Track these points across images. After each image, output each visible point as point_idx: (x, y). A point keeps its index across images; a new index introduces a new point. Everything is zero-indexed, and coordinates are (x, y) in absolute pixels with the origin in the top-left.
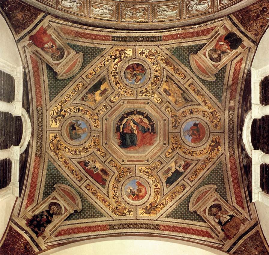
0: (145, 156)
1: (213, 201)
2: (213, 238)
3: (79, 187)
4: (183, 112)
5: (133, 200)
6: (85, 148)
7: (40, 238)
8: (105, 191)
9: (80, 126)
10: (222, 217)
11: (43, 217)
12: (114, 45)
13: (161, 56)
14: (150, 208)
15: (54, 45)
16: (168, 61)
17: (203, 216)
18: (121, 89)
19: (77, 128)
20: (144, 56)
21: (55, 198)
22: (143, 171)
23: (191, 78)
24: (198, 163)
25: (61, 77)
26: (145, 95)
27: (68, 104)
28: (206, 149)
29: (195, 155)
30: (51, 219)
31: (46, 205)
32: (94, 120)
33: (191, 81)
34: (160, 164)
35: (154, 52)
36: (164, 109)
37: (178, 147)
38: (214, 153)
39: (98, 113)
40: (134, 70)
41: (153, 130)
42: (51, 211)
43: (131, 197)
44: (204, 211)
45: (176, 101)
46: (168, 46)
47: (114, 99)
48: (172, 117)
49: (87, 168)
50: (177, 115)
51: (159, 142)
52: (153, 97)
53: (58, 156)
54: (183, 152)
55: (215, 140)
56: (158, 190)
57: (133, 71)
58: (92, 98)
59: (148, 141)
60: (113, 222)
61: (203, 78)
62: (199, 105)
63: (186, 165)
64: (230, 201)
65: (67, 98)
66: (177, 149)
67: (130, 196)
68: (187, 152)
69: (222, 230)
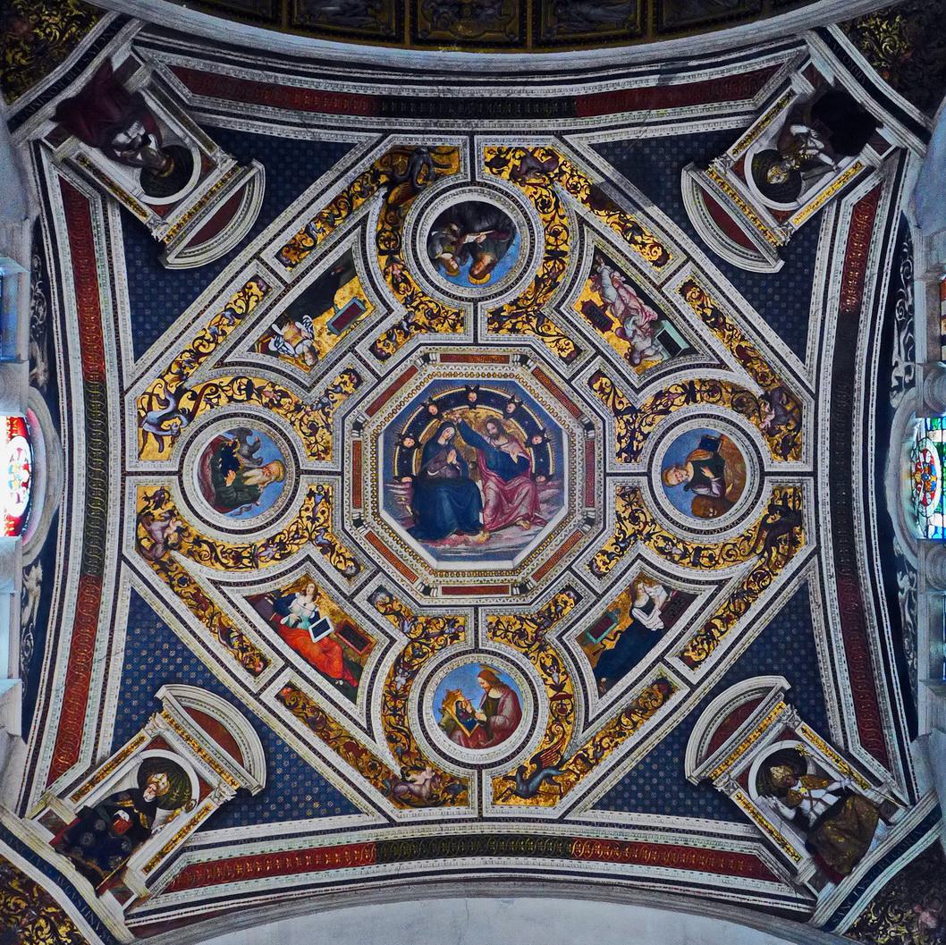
0: (514, 571)
3: (256, 696)
4: (659, 395)
5: (467, 746)
6: (277, 540)
8: (356, 711)
9: (254, 456)
10: (810, 798)
13: (572, 176)
14: (534, 775)
15: (152, 138)
18: (415, 304)
19: (244, 462)
20: (506, 175)
21: (159, 742)
22: (507, 631)
24: (718, 590)
25: (180, 261)
26: (510, 326)
27: (208, 363)
28: (748, 539)
29: (705, 561)
30: (150, 824)
32: (310, 428)
33: (684, 276)
34: (572, 601)
35: (545, 159)
37: (640, 532)
38: (778, 552)
39: (325, 400)
41: (543, 468)
42: (146, 794)
43: (459, 733)
44: (743, 780)
45: (633, 349)
46: (601, 138)
47: (388, 345)
48: (618, 413)
49: (283, 621)
50: (638, 406)
51: (569, 514)
52: (543, 334)
53: (168, 576)
54: (661, 551)
55: (780, 503)
57: (463, 235)
58: (301, 342)
59: (523, 511)
62: (722, 365)
65: (205, 343)
66: (639, 541)
67: (457, 728)
69: (809, 847)
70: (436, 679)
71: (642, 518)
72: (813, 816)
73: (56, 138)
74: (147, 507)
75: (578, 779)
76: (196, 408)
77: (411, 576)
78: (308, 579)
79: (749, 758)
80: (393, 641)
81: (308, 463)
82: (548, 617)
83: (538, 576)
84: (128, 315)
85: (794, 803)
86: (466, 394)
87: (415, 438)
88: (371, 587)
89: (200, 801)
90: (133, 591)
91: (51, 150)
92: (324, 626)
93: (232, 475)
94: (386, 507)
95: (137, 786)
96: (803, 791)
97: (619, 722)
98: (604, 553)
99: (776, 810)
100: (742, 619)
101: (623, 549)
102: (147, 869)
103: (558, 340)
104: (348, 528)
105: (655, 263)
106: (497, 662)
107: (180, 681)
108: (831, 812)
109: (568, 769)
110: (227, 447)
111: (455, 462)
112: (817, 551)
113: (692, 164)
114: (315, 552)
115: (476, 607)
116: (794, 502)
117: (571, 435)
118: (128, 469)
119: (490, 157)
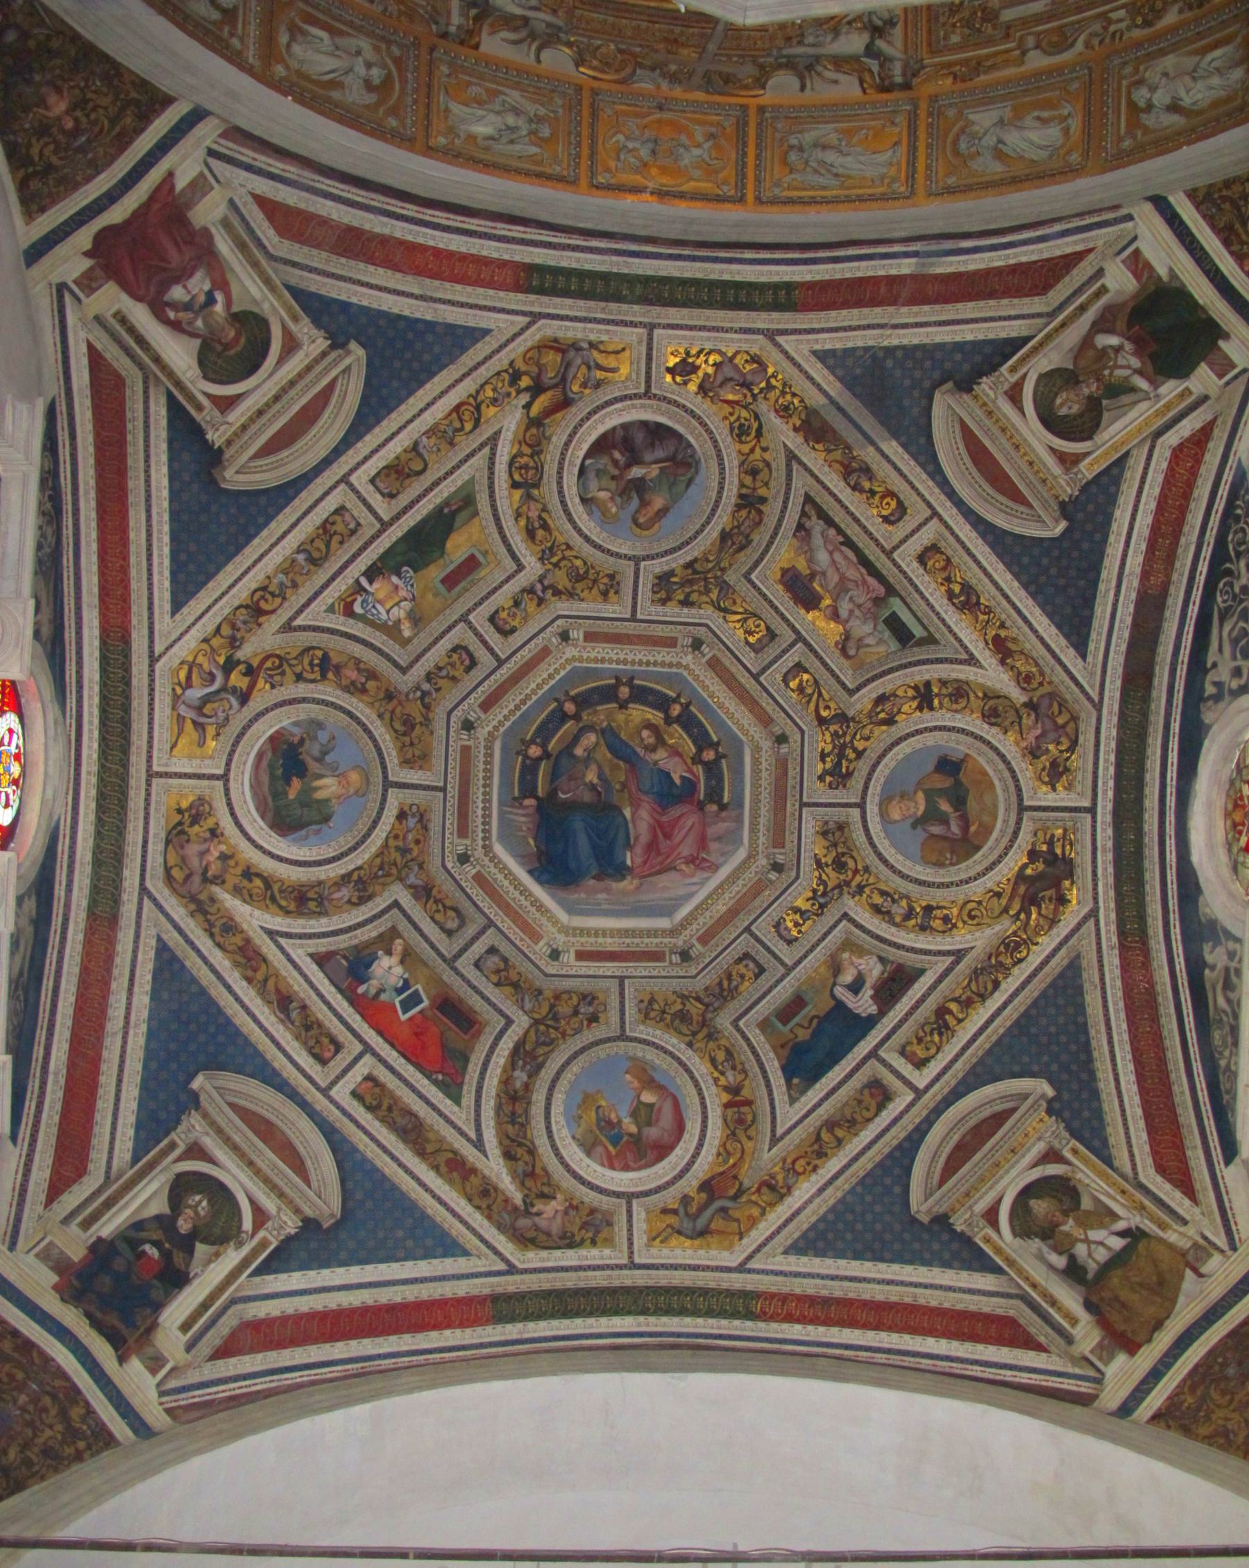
0: (673, 932)
1: (1035, 1165)
2: (1040, 1348)
3: (325, 1092)
4: (881, 699)
5: (612, 1167)
6: (355, 877)
7: (135, 1364)
9: (328, 759)
10: (1087, 1241)
11: (144, 1252)
12: (535, 317)
13: (783, 393)
14: (702, 1209)
15: (219, 297)
16: (816, 424)
17: (987, 1240)
18: (554, 560)
19: (313, 766)
20: (692, 387)
21: (196, 1151)
22: (664, 1012)
23: (935, 520)
24: (957, 962)
25: (241, 478)
26: (681, 597)
27: (273, 623)
28: (998, 895)
29: (937, 924)
30: (188, 1265)
31: (154, 1186)
32: (404, 724)
33: (926, 536)
34: (749, 974)
35: (748, 367)
36: (779, 677)
37: (848, 884)
38: (1039, 914)
39: (426, 686)
40: (635, 460)
41: (715, 794)
42: (180, 1222)
43: (599, 1149)
44: (991, 1216)
45: (847, 636)
46: (828, 342)
47: (514, 615)
48: (822, 721)
49: (361, 990)
50: (851, 713)
51: (749, 857)
52: (725, 610)
53: (207, 920)
54: (877, 909)
55: (1044, 848)
56: (745, 1109)
57: (628, 466)
58: (397, 604)
59: (686, 850)
60: (511, 1284)
61: (1000, 521)
62: (971, 660)
63: (892, 978)
64: (1122, 1159)
65: (268, 596)
66: (846, 896)
68: (899, 910)
69: (1089, 1306)
70: (568, 1076)
71: (851, 864)
72: (1092, 1267)
73: (88, 283)
74: (180, 823)
75: (763, 1214)
76: (252, 686)
77: (535, 936)
78: (393, 933)
79: (999, 1187)
80: (509, 1022)
81: (398, 774)
82: (724, 992)
83: (704, 940)
84: (167, 550)
85: (1063, 1246)
86: (615, 688)
87: (544, 746)
88: (478, 948)
89: (253, 1235)
90: (159, 939)
91: (79, 300)
92: (415, 999)
93: (296, 783)
94: (502, 838)
95: (167, 1211)
96: (1078, 1233)
97: (818, 1138)
98: (797, 910)
99: (1040, 1257)
100: (988, 1002)
101: (822, 906)
102: (185, 1327)
103: (745, 620)
104: (449, 865)
105: (886, 519)
106: (650, 1055)
107: (222, 1067)
108: (1118, 1260)
109: (750, 1201)
110: (291, 745)
111: (595, 781)
112: (1094, 913)
113: (950, 385)
114: (406, 899)
115: (621, 979)
116: (1063, 847)
117: (757, 749)
118: (156, 768)
119: (672, 361)
